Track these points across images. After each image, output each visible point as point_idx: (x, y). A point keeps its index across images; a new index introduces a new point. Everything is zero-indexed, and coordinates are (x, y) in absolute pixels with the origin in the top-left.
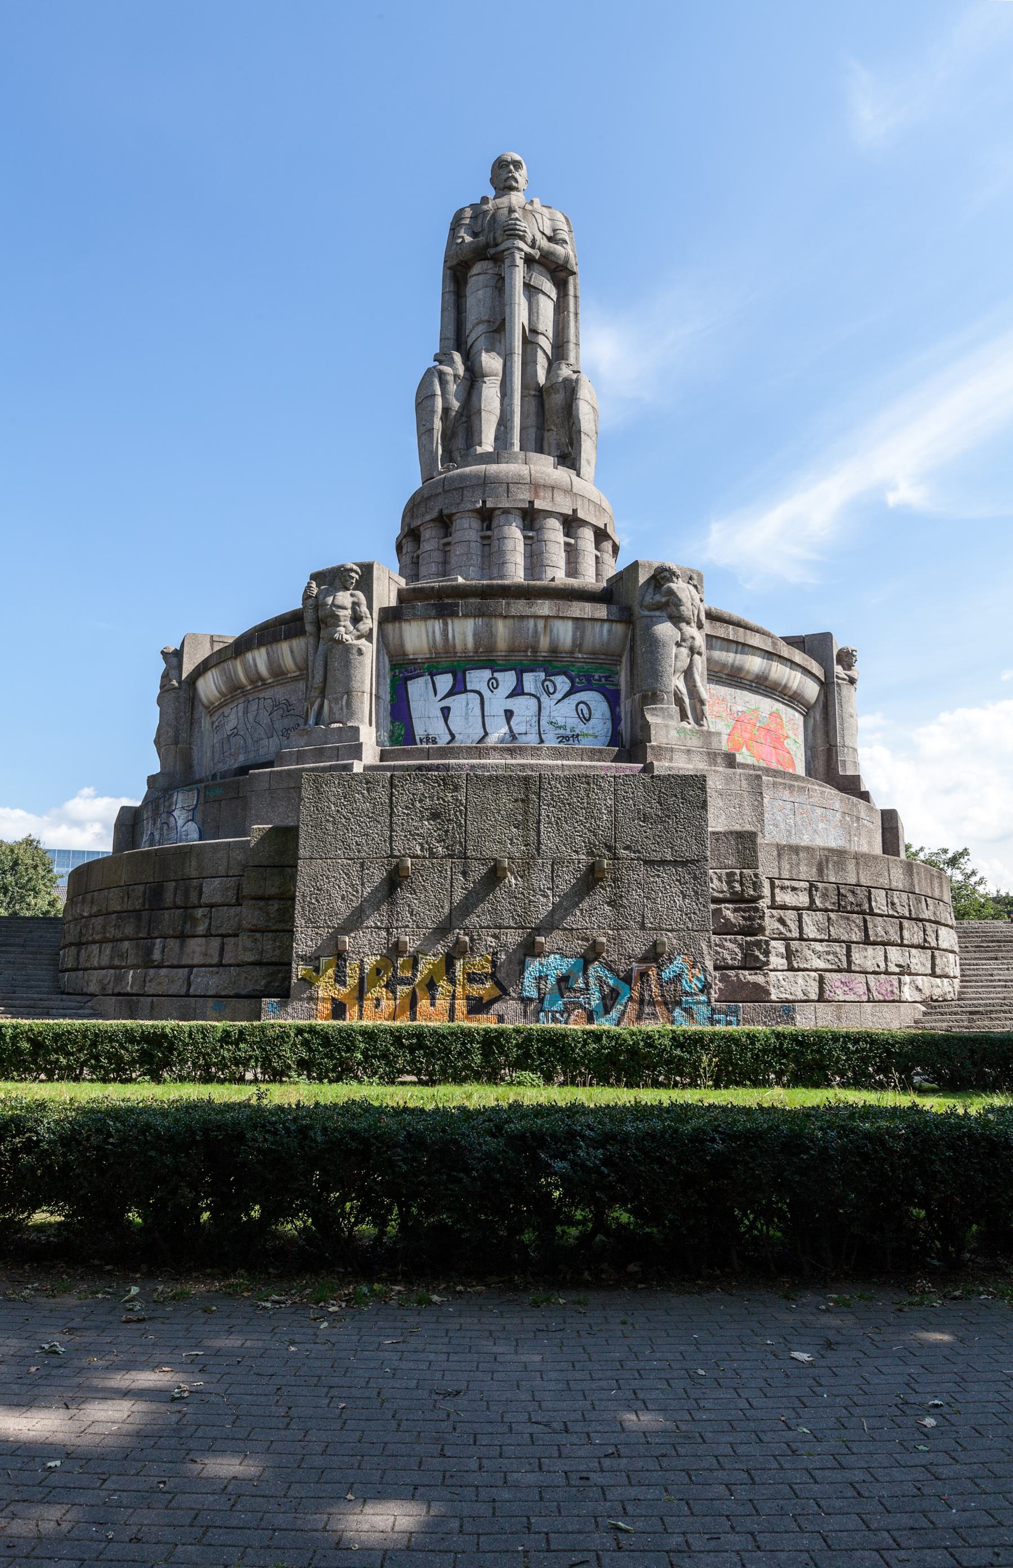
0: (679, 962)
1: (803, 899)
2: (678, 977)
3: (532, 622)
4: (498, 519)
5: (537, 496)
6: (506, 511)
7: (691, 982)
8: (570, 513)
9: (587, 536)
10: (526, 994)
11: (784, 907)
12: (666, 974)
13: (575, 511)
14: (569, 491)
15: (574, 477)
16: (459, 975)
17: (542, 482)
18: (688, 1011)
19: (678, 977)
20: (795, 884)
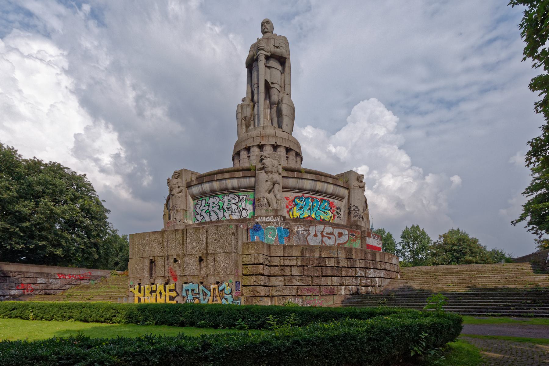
0: (225, 285)
1: (294, 263)
2: (224, 289)
3: (224, 182)
4: (252, 150)
5: (263, 140)
6: (253, 146)
7: (227, 291)
8: (274, 143)
9: (268, 150)
10: (183, 295)
11: (285, 266)
12: (221, 288)
13: (276, 143)
14: (275, 136)
15: (279, 132)
16: (167, 290)
17: (264, 135)
18: (226, 299)
19: (224, 289)
20: (290, 258)
